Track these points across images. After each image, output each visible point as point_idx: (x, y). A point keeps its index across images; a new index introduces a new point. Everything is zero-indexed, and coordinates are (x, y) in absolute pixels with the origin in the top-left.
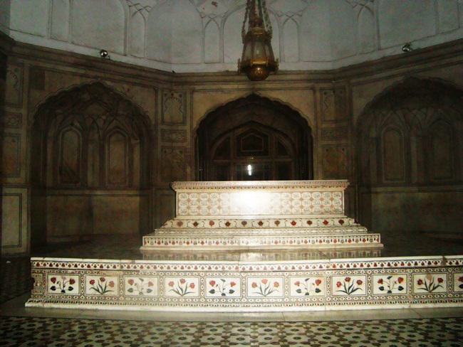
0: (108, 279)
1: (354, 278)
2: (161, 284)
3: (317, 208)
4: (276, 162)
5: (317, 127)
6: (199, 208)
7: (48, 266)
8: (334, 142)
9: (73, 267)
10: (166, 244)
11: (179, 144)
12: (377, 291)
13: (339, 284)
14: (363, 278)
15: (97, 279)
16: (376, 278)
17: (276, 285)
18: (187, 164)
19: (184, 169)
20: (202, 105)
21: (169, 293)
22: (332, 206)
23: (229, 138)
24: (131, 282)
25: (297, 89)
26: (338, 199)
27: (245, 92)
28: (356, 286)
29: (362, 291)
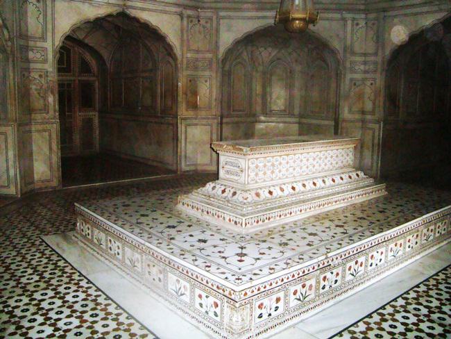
0: (308, 283)
4: (79, 81)
6: (265, 174)
7: (256, 292)
9: (280, 283)
10: (263, 221)
11: (39, 66)
15: (299, 287)
18: (50, 93)
19: (45, 98)
20: (65, 20)
22: (347, 161)
24: (325, 278)
25: (165, 12)
26: (350, 154)
27: (115, 9)
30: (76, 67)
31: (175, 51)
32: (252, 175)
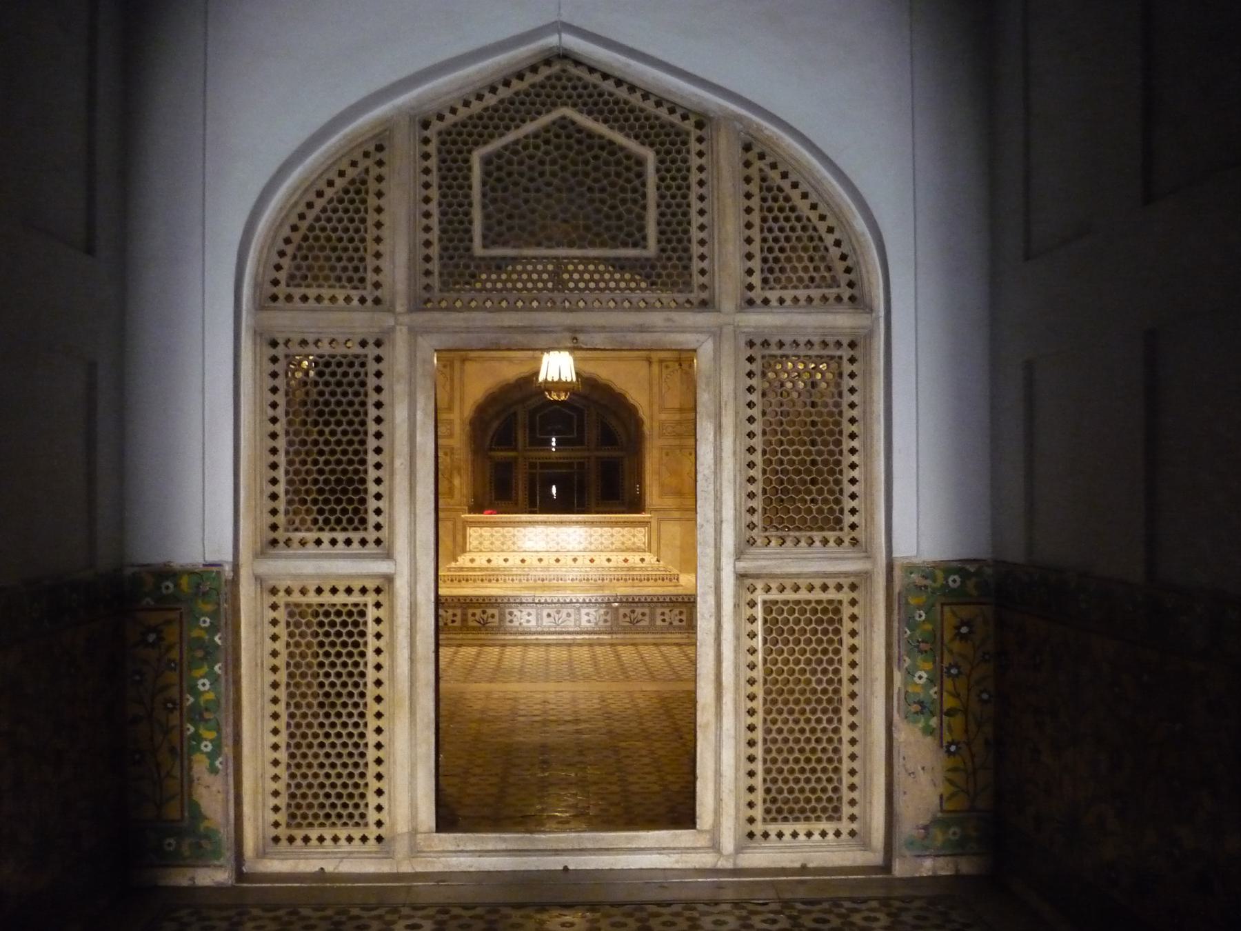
1: (639, 611)
2: (464, 615)
3: (618, 544)
4: (597, 458)
5: (652, 418)
8: (677, 442)
12: (659, 622)
13: (625, 616)
14: (647, 611)
16: (659, 611)
17: (569, 615)
18: (455, 473)
21: (472, 623)
23: (515, 414)
28: (640, 617)
29: (645, 622)
30: (592, 434)
31: (641, 413)
32: (475, 543)
